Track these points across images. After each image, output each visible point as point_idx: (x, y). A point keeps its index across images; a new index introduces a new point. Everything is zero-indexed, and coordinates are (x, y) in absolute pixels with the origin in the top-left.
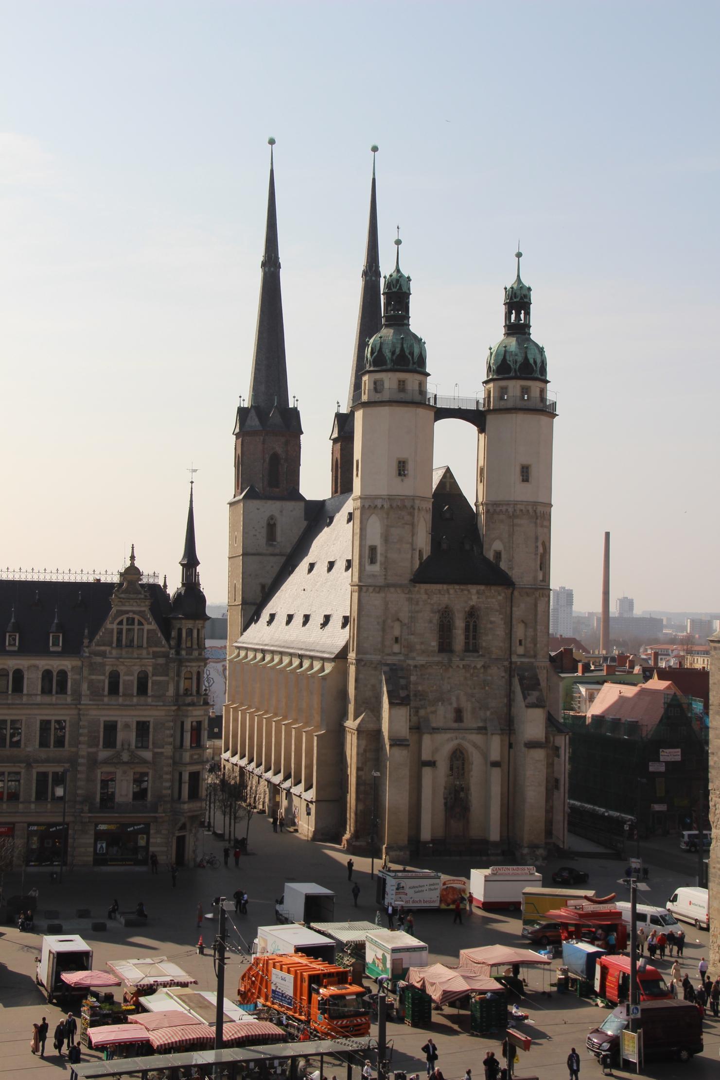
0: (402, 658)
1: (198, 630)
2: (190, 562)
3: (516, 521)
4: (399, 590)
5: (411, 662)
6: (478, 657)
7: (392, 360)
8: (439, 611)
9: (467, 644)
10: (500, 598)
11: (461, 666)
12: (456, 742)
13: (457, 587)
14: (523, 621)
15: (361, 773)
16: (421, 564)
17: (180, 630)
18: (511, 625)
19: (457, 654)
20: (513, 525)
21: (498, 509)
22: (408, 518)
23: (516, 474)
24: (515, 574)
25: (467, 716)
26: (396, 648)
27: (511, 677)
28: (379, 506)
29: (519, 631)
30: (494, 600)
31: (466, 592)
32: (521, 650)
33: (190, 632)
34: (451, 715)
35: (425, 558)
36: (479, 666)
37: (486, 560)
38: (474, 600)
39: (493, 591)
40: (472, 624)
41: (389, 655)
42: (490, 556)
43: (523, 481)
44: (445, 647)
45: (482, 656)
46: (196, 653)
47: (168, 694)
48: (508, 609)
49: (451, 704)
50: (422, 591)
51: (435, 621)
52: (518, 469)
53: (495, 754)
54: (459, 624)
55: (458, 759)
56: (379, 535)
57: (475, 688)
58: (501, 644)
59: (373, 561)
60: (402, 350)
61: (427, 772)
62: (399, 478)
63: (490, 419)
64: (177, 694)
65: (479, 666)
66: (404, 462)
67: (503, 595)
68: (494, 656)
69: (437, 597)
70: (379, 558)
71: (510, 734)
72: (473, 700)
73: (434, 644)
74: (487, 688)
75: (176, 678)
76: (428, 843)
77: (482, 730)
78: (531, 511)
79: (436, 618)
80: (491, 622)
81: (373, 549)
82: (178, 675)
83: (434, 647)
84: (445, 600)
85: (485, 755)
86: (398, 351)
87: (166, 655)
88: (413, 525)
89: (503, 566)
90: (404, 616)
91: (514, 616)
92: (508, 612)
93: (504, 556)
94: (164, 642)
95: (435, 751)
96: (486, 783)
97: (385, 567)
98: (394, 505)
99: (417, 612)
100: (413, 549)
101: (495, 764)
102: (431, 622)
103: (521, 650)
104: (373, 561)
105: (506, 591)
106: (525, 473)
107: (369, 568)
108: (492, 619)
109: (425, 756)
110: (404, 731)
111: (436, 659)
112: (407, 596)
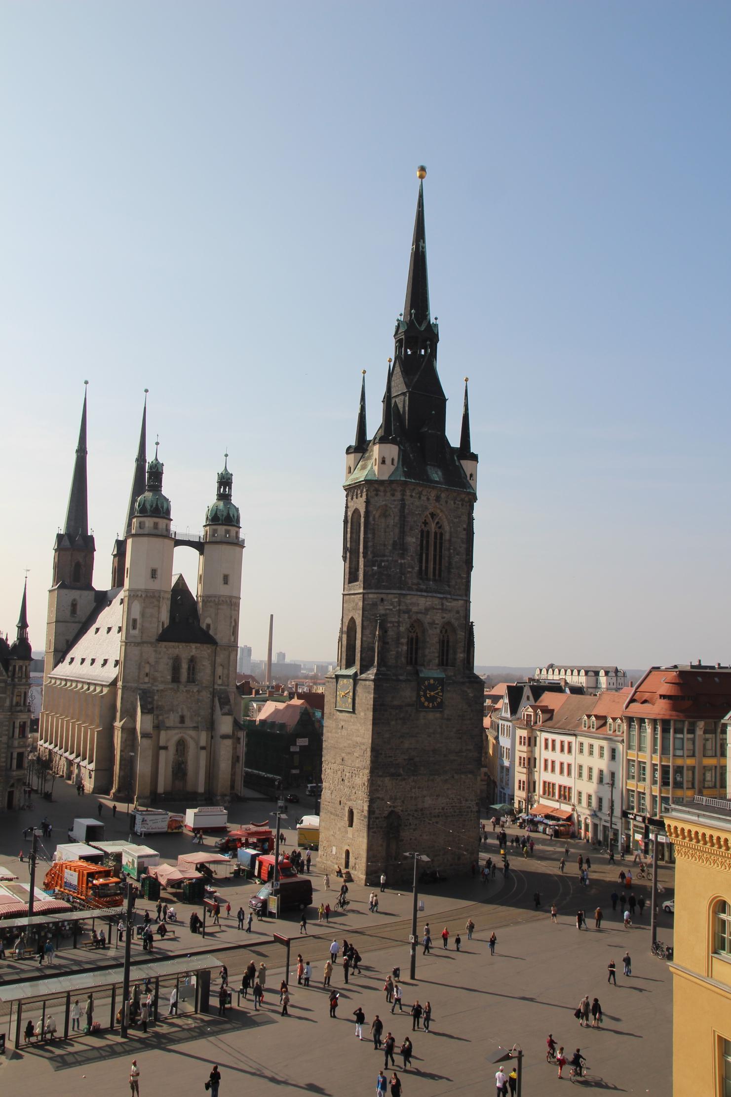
0: (149, 685)
1: (26, 667)
2: (23, 625)
3: (219, 607)
4: (149, 645)
5: (155, 688)
7: (151, 511)
9: (188, 678)
10: (209, 651)
12: (180, 735)
13: (184, 644)
14: (221, 665)
15: (122, 753)
16: (163, 630)
17: (15, 667)
20: (218, 609)
21: (209, 600)
22: (156, 603)
23: (220, 580)
24: (218, 638)
25: (187, 720)
26: (146, 680)
27: (214, 697)
28: (140, 595)
29: (219, 671)
31: (189, 647)
32: (220, 682)
33: (21, 667)
34: (178, 719)
35: (165, 627)
36: (195, 691)
37: (202, 629)
38: (194, 652)
40: (192, 666)
41: (142, 683)
42: (204, 627)
43: (224, 584)
44: (176, 679)
45: (197, 685)
46: (24, 681)
47: (5, 705)
48: (213, 658)
49: (178, 713)
50: (163, 646)
51: (170, 664)
52: (222, 576)
53: (203, 743)
54: (184, 666)
55: (181, 745)
56: (139, 613)
59: (134, 628)
60: (157, 505)
61: (162, 753)
62: (153, 579)
63: (206, 547)
64: (11, 706)
65: (195, 691)
66: (155, 570)
67: (211, 649)
68: (204, 685)
70: (138, 626)
71: (212, 730)
73: (169, 677)
75: (11, 695)
76: (161, 794)
77: (196, 728)
78: (228, 601)
79: (171, 662)
80: (203, 665)
81: (135, 621)
82: (13, 694)
84: (177, 651)
85: (197, 743)
86: (154, 505)
87: (5, 681)
88: (159, 607)
89: (211, 632)
90: (152, 660)
91: (216, 662)
92: (213, 659)
93: (212, 627)
94: (4, 673)
95: (168, 740)
96: (197, 759)
97: (142, 632)
98: (149, 595)
99: (160, 658)
100: (159, 622)
101: (203, 748)
102: (167, 664)
103: (220, 682)
104: (134, 628)
106: (226, 580)
107: (132, 632)
108: (204, 663)
109: (162, 743)
110: (149, 728)
111: (170, 686)
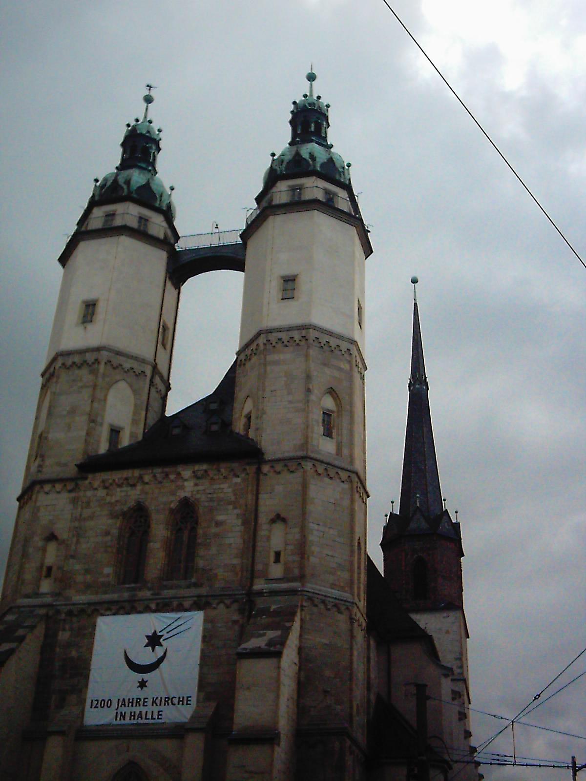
4: (58, 487)
6: (188, 587)
8: (124, 514)
10: (237, 480)
13: (158, 471)
20: (265, 365)
26: (46, 586)
30: (225, 486)
32: (277, 571)
41: (27, 596)
45: (196, 585)
50: (96, 484)
51: (115, 532)
54: (160, 531)
58: (236, 561)
69: (121, 491)
73: (108, 570)
79: (115, 526)
80: (218, 524)
83: (108, 575)
84: (134, 494)
90: (62, 529)
105: (248, 467)
108: (220, 518)
112: (73, 495)
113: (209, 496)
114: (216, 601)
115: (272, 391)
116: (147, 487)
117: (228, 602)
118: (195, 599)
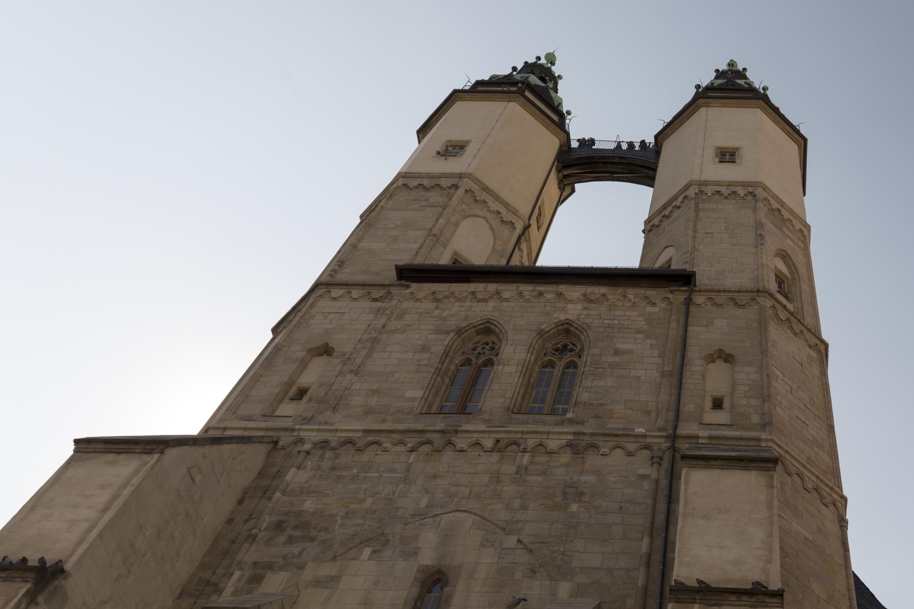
11: (488, 443)
18: (683, 356)
19: (486, 416)
30: (634, 313)
39: (631, 297)
57: (524, 508)
72: (511, 541)
74: (574, 507)
83: (413, 400)
84: (480, 311)
113: (606, 322)
114: (610, 444)
115: (706, 233)
116: (506, 304)
117: (631, 447)
118: (571, 437)
